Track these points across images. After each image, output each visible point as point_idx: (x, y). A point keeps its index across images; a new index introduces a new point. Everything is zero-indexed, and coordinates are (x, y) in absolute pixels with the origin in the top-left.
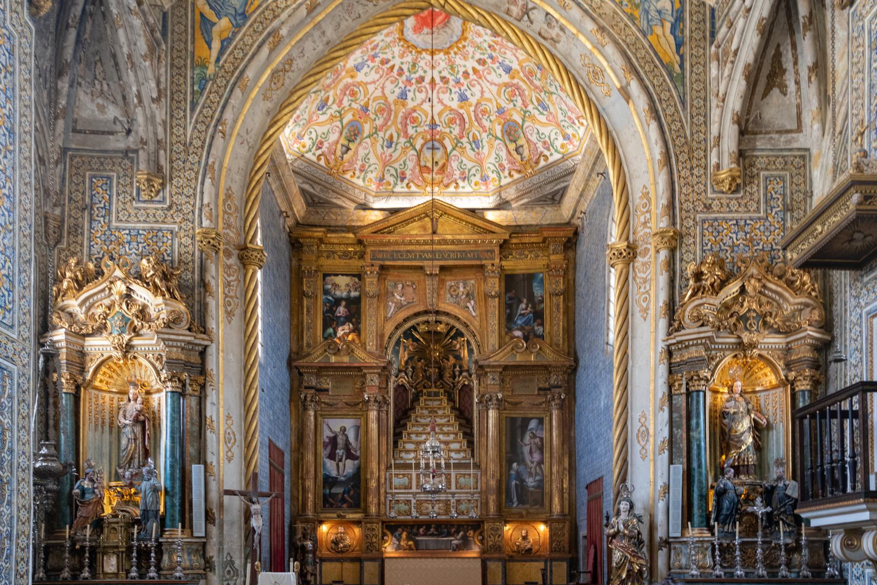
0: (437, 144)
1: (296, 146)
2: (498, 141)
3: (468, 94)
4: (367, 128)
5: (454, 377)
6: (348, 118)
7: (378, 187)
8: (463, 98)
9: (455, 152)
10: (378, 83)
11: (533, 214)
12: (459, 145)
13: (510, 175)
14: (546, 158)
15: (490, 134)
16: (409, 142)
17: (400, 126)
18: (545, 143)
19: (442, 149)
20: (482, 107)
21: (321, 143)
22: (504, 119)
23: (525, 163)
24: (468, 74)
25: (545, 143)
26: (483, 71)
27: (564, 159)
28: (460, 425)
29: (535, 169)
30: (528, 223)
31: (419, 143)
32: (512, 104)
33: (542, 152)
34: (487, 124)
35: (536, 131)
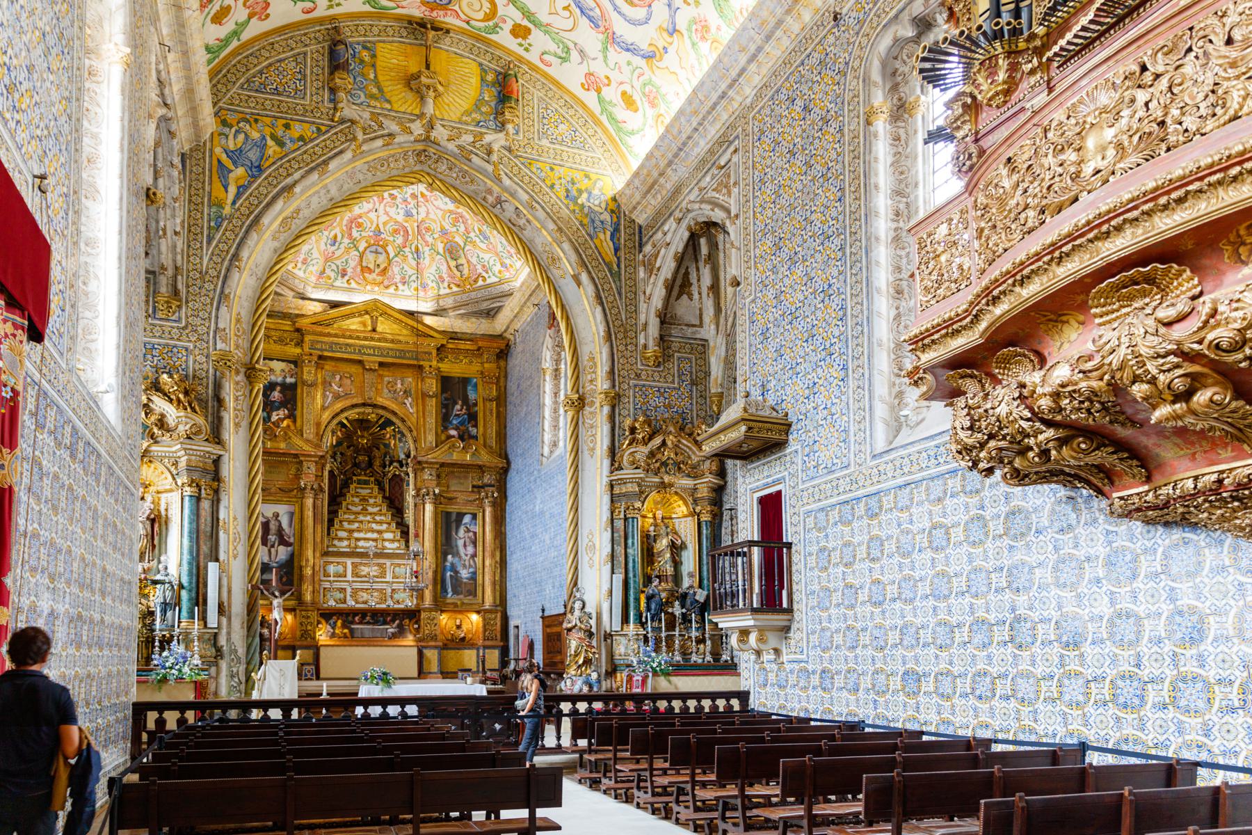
0: (380, 250)
14: (484, 279)
27: (500, 282)
28: (393, 515)
34: (430, 240)
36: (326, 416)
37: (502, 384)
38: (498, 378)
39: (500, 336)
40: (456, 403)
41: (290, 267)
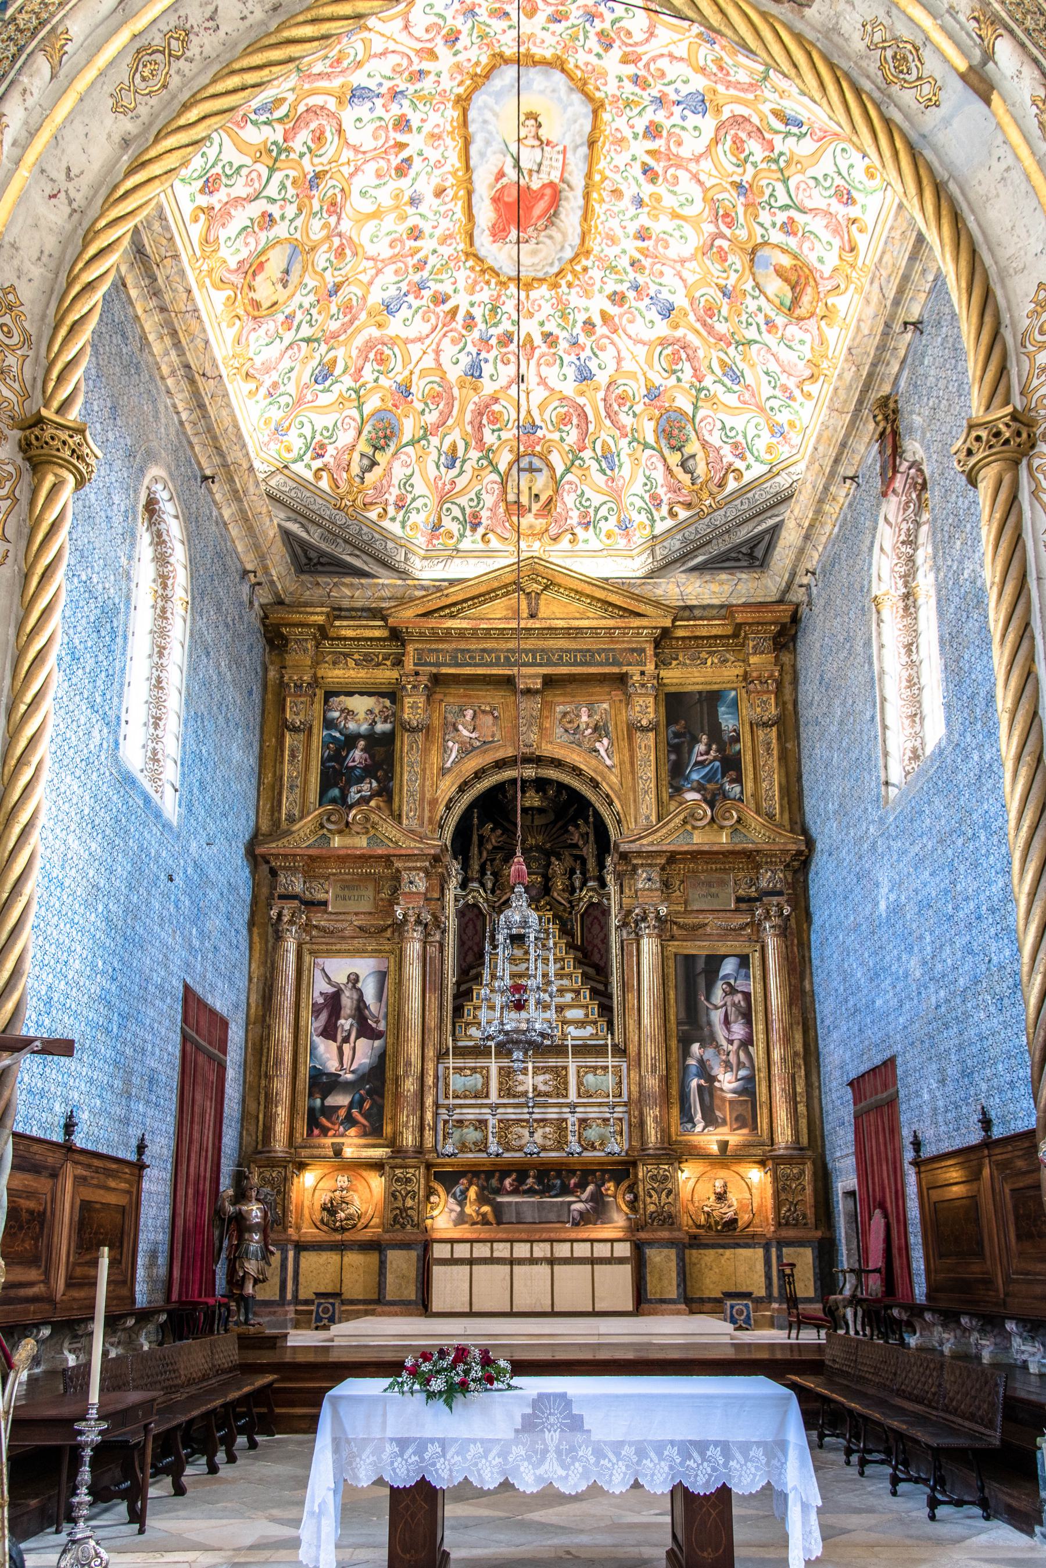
3: (593, 365)
5: (572, 891)
8: (585, 376)
10: (428, 341)
11: (714, 587)
13: (672, 514)
15: (634, 440)
17: (469, 428)
20: (620, 391)
24: (594, 326)
26: (621, 316)
30: (705, 602)
31: (504, 460)
36: (447, 787)
37: (788, 697)
38: (779, 684)
39: (781, 601)
40: (696, 740)
41: (373, 515)
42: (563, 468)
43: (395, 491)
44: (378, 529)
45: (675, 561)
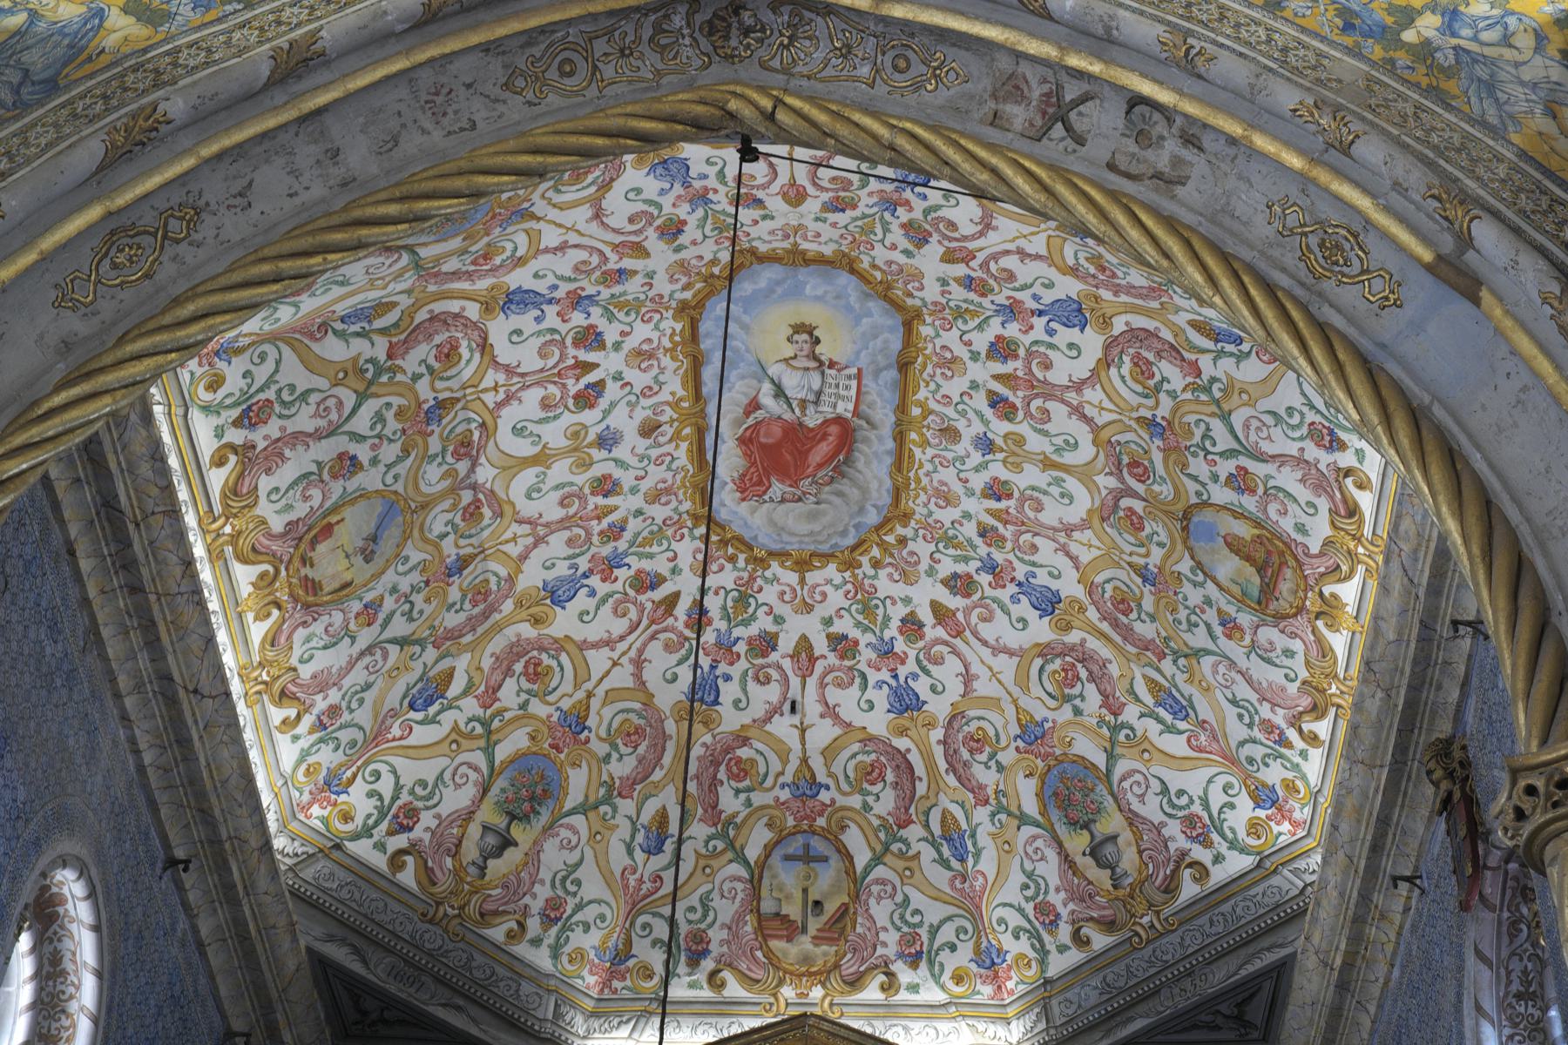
0: (818, 845)
1: (316, 810)
2: (1028, 831)
4: (578, 783)
6: (513, 743)
7: (606, 984)
9: (880, 871)
12: (895, 847)
14: (1202, 872)
15: (1001, 809)
16: (723, 835)
18: (1190, 821)
19: (835, 862)
21: (412, 813)
22: (1045, 757)
23: (1128, 895)
25: (1190, 821)
27: (1265, 867)
29: (1167, 911)
31: (756, 841)
32: (1067, 708)
33: (1184, 854)
34: (987, 777)
35: (1155, 786)
41: (497, 933)
42: (869, 855)
43: (543, 892)
44: (505, 959)
45: (1091, 1028)
